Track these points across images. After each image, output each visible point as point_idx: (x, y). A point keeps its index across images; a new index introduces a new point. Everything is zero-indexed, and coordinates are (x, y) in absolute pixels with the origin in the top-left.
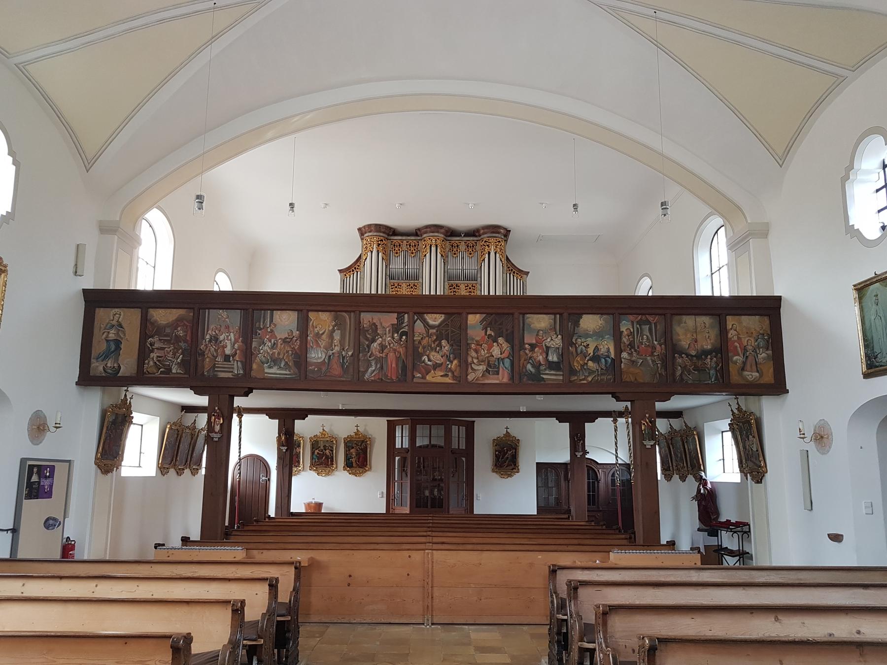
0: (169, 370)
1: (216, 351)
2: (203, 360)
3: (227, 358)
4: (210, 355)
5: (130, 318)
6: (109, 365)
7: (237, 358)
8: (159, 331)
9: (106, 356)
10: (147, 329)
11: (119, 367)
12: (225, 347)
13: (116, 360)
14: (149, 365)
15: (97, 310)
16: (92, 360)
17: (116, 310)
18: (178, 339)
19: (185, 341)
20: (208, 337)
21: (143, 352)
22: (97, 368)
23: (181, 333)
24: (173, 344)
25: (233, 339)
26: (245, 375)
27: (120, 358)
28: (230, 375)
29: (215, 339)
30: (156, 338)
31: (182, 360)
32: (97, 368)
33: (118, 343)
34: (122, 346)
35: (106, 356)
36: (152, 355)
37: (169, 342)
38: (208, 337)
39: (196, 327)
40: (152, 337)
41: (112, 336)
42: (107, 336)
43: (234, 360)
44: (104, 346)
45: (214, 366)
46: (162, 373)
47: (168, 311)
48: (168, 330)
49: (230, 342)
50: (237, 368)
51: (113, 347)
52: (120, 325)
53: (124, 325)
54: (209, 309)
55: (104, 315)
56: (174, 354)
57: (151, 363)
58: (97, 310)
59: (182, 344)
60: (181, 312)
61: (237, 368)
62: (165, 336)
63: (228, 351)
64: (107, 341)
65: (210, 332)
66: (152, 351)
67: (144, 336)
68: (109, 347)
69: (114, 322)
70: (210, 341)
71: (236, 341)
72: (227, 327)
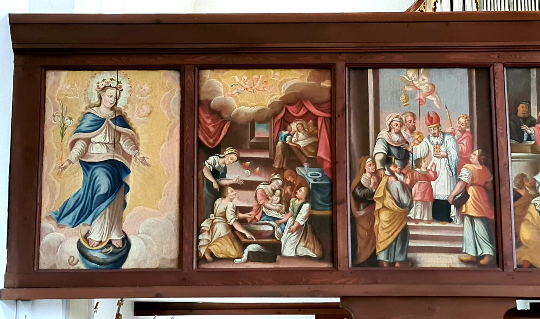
0: (272, 250)
1: (407, 188)
2: (371, 218)
3: (440, 210)
4: (389, 202)
5: (150, 98)
6: (95, 236)
7: (470, 208)
8: (237, 134)
9: (83, 209)
10: (202, 133)
11: (126, 243)
12: (429, 178)
13: (117, 220)
14: (215, 238)
15: (51, 77)
16: (46, 224)
17: (107, 76)
18: (293, 157)
19: (315, 163)
20: (379, 149)
21: (194, 200)
22: (60, 246)
23: (298, 136)
24: (280, 171)
25: (454, 155)
26: (500, 258)
27: (127, 215)
28: (450, 261)
29: (400, 155)
30: (228, 158)
31: (311, 218)
32: (60, 246)
33: (117, 171)
34: (131, 180)
35: (83, 209)
36: (220, 205)
37: (266, 165)
38: (379, 149)
39: (342, 118)
40: (217, 150)
41: (99, 152)
42: (85, 152)
43: (462, 216)
44: (74, 183)
45: (404, 235)
46: (253, 257)
47: (260, 75)
48: (262, 132)
49: (446, 161)
50: (473, 239)
51: (103, 184)
52: (121, 120)
53: (132, 118)
54: (376, 67)
55: (69, 91)
56: (285, 201)
57: (220, 229)
58: (51, 77)
59: (306, 172)
60: (294, 79)
61: (473, 239)
62: (256, 147)
63: (442, 189)
64: (87, 166)
65: (383, 133)
66: (220, 193)
67: (193, 152)
68: (91, 184)
69: (104, 112)
70: (387, 161)
71: (463, 160)
72: (434, 120)
